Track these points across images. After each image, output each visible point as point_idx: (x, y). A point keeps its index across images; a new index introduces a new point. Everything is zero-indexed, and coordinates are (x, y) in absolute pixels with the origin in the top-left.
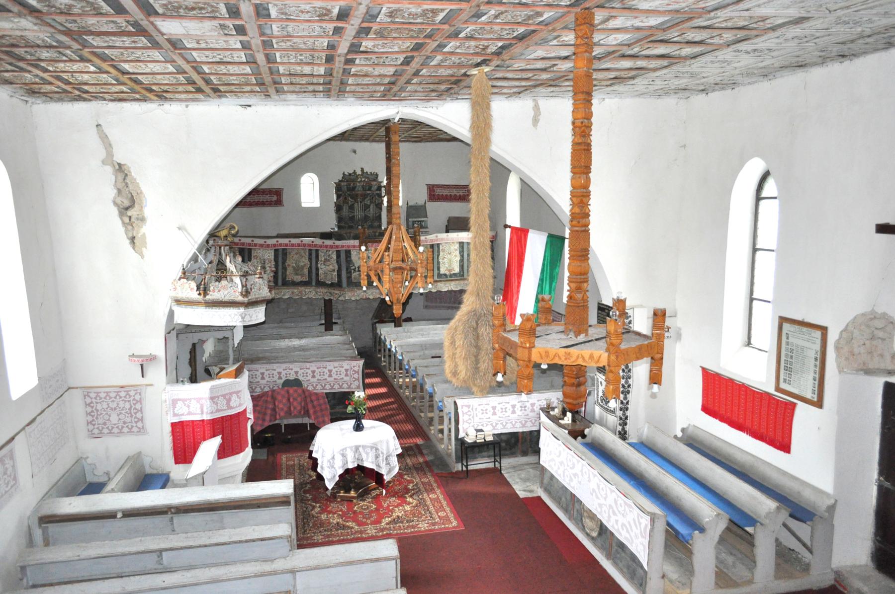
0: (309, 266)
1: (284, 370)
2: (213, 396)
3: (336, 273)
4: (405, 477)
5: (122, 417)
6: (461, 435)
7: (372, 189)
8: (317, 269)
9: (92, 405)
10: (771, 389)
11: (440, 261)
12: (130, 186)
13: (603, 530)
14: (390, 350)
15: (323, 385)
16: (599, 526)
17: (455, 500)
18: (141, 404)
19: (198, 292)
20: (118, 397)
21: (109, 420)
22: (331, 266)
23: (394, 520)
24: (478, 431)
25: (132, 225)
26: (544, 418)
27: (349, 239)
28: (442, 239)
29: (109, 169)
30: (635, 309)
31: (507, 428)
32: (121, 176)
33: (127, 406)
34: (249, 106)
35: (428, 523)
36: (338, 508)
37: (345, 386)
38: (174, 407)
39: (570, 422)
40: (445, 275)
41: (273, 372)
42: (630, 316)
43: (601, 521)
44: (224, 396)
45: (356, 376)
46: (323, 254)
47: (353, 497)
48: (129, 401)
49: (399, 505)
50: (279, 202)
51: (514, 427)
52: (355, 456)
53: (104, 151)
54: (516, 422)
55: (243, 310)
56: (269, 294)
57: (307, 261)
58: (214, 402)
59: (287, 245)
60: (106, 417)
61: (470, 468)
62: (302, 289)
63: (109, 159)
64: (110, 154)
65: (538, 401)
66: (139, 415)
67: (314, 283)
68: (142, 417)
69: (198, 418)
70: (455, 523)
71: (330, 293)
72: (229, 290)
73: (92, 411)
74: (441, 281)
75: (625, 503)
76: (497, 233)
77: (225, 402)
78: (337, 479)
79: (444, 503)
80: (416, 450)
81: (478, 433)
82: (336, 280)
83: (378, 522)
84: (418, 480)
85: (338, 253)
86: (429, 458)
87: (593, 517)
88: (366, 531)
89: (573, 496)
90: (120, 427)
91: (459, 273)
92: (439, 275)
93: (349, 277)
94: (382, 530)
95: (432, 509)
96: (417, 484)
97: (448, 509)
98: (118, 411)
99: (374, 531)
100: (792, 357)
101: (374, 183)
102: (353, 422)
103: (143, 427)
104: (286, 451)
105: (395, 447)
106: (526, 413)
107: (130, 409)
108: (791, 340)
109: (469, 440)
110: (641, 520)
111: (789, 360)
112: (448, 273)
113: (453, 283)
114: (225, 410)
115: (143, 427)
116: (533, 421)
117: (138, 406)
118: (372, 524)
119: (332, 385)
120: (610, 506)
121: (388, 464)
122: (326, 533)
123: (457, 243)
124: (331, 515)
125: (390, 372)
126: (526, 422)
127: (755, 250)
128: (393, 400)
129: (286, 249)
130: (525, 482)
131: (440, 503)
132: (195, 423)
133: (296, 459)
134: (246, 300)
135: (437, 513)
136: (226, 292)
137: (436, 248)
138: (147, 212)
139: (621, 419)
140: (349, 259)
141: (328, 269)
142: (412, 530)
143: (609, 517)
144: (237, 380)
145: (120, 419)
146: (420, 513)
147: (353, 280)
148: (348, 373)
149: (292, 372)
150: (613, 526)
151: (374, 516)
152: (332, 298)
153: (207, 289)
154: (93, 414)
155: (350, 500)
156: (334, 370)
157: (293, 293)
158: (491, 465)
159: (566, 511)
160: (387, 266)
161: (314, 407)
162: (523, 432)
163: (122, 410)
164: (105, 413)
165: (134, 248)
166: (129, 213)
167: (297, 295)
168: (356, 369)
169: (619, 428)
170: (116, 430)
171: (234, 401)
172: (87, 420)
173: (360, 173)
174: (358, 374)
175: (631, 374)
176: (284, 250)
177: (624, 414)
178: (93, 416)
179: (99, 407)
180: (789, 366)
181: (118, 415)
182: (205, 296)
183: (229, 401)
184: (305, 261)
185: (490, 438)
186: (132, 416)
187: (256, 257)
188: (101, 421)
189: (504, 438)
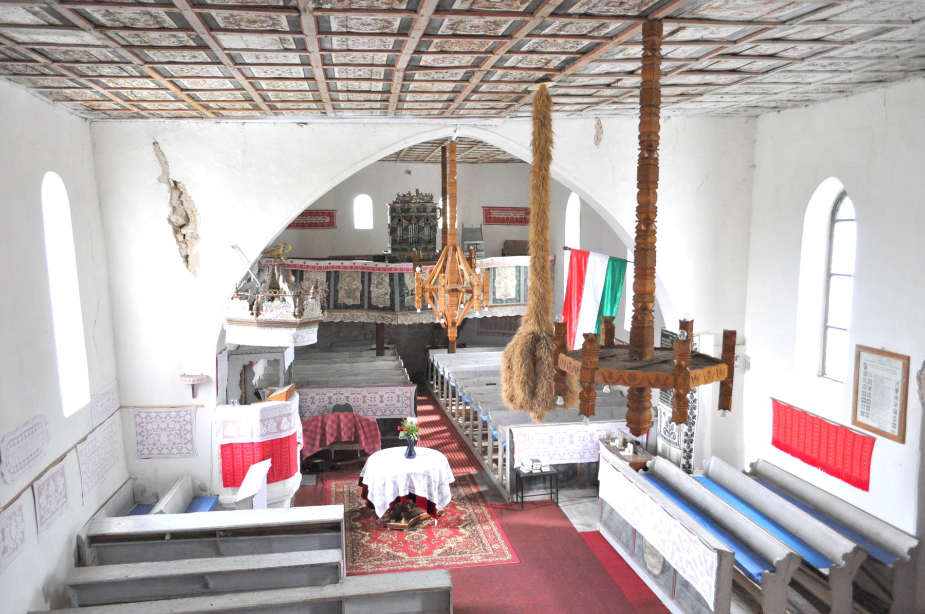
0: (361, 289)
1: (334, 394)
2: (263, 418)
3: (388, 297)
4: (458, 507)
5: (172, 437)
6: (516, 466)
7: (427, 211)
8: (370, 292)
9: (142, 425)
10: (847, 422)
11: (496, 285)
12: (184, 203)
13: (666, 567)
14: (442, 377)
15: (374, 411)
16: (662, 563)
17: (511, 534)
18: (191, 425)
19: (250, 312)
20: (168, 418)
21: (159, 440)
22: (384, 290)
23: (446, 551)
24: (534, 461)
25: (186, 243)
26: (603, 450)
27: (403, 261)
28: (498, 263)
29: (165, 187)
30: (701, 336)
31: (565, 459)
32: (176, 194)
33: (178, 426)
34: (306, 124)
35: (481, 556)
36: (388, 537)
37: (397, 412)
38: (224, 430)
39: (631, 453)
40: (501, 300)
41: (324, 396)
42: (696, 344)
43: (664, 558)
44: (274, 419)
45: (408, 402)
46: (376, 277)
47: (404, 527)
48: (179, 422)
49: (451, 536)
50: (331, 224)
51: (572, 458)
52: (406, 484)
53: (160, 169)
54: (574, 453)
55: (296, 331)
56: (322, 315)
57: (359, 284)
58: (264, 425)
59: (339, 267)
60: (157, 438)
61: (526, 499)
62: (354, 312)
63: (165, 177)
64: (166, 172)
65: (598, 431)
66: (189, 436)
67: (366, 306)
68: (192, 438)
69: (247, 440)
70: (509, 556)
71: (383, 318)
72: (282, 310)
73: (143, 431)
74: (496, 306)
75: (691, 539)
76: (555, 257)
77: (275, 425)
78: (388, 507)
79: (499, 535)
80: (468, 479)
81: (535, 463)
82: (388, 304)
83: (429, 553)
84: (471, 510)
85: (391, 275)
86: (483, 488)
87: (655, 553)
88: (417, 561)
89: (634, 531)
90: (170, 448)
91: (516, 299)
92: (495, 300)
93: (402, 301)
94: (433, 561)
95: (485, 541)
96: (470, 515)
97: (502, 542)
98: (167, 432)
99: (425, 562)
100: (870, 389)
101: (429, 205)
102: (404, 449)
103: (192, 448)
104: (337, 478)
105: (449, 476)
106: (585, 443)
107: (180, 430)
108: (869, 370)
109: (525, 470)
110: (707, 557)
111: (868, 391)
112: (503, 298)
113: (509, 308)
114: (275, 433)
115: (192, 448)
116: (592, 452)
117: (188, 427)
118: (423, 554)
119: (383, 411)
120: (674, 543)
121: (440, 493)
122: (376, 563)
123: (514, 266)
124: (381, 545)
125: (443, 399)
126: (585, 453)
127: (829, 275)
128: (445, 428)
129: (338, 271)
130: (583, 515)
131: (494, 535)
132: (244, 446)
133: (345, 486)
134: (298, 320)
135: (491, 545)
136: (278, 312)
137: (492, 272)
138: (201, 231)
139: (685, 451)
140: (402, 282)
141: (380, 292)
142: (465, 562)
143: (673, 554)
144: (288, 402)
145: (169, 440)
146: (473, 545)
148: (400, 399)
149: (343, 397)
150: (676, 564)
151: (426, 547)
152: (384, 322)
153: (260, 309)
154: (142, 434)
155: (400, 530)
156: (386, 396)
157: (344, 316)
158: (547, 498)
159: (626, 546)
160: (442, 288)
161: (364, 433)
162: (581, 464)
163: (172, 430)
164: (155, 433)
165: (187, 267)
166: (184, 231)
167: (349, 318)
168: (408, 395)
169: (684, 461)
170: (165, 451)
171: (284, 426)
172: (137, 441)
173: (415, 194)
174: (410, 400)
175: (697, 405)
176: (336, 272)
177: (689, 447)
178: (143, 436)
179: (149, 427)
180: (867, 398)
181: (168, 436)
182: (257, 315)
183: (279, 424)
184: (358, 284)
185: (546, 469)
186: (181, 437)
187: (308, 280)
188: (151, 442)
189: (561, 469)
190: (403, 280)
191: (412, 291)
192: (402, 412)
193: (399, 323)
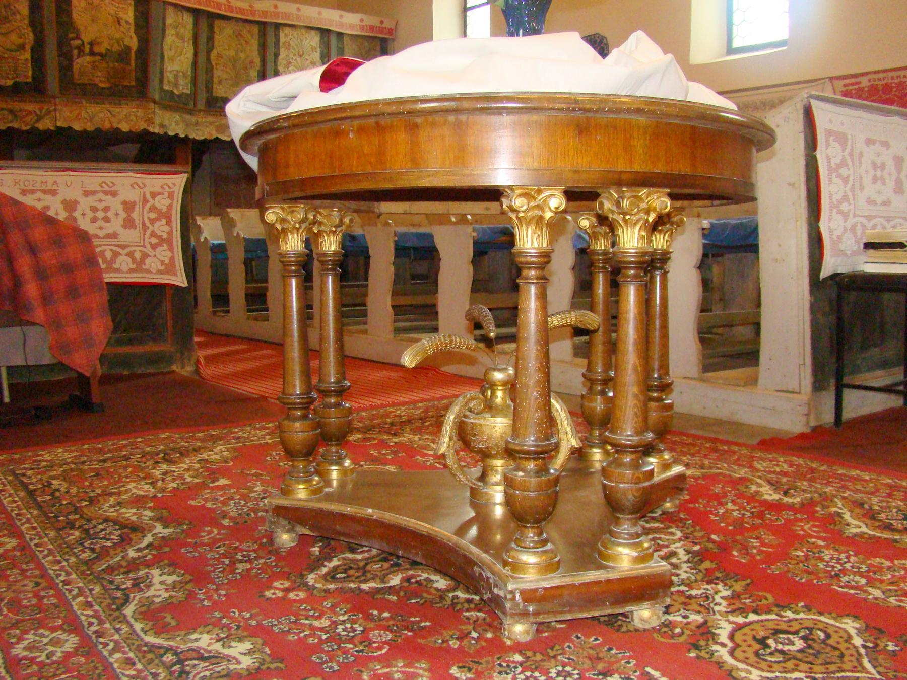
3: (27, 55)
28: (287, 15)
45: (161, 228)
71: (11, 111)
82: (28, 74)
93: (66, 69)
147: (76, 76)
148: (135, 215)
152: (16, 125)
161: (41, 274)
168: (162, 203)
174: (169, 223)
190: (69, 13)
191: (91, 44)
192: (142, 261)
193: (59, 124)
